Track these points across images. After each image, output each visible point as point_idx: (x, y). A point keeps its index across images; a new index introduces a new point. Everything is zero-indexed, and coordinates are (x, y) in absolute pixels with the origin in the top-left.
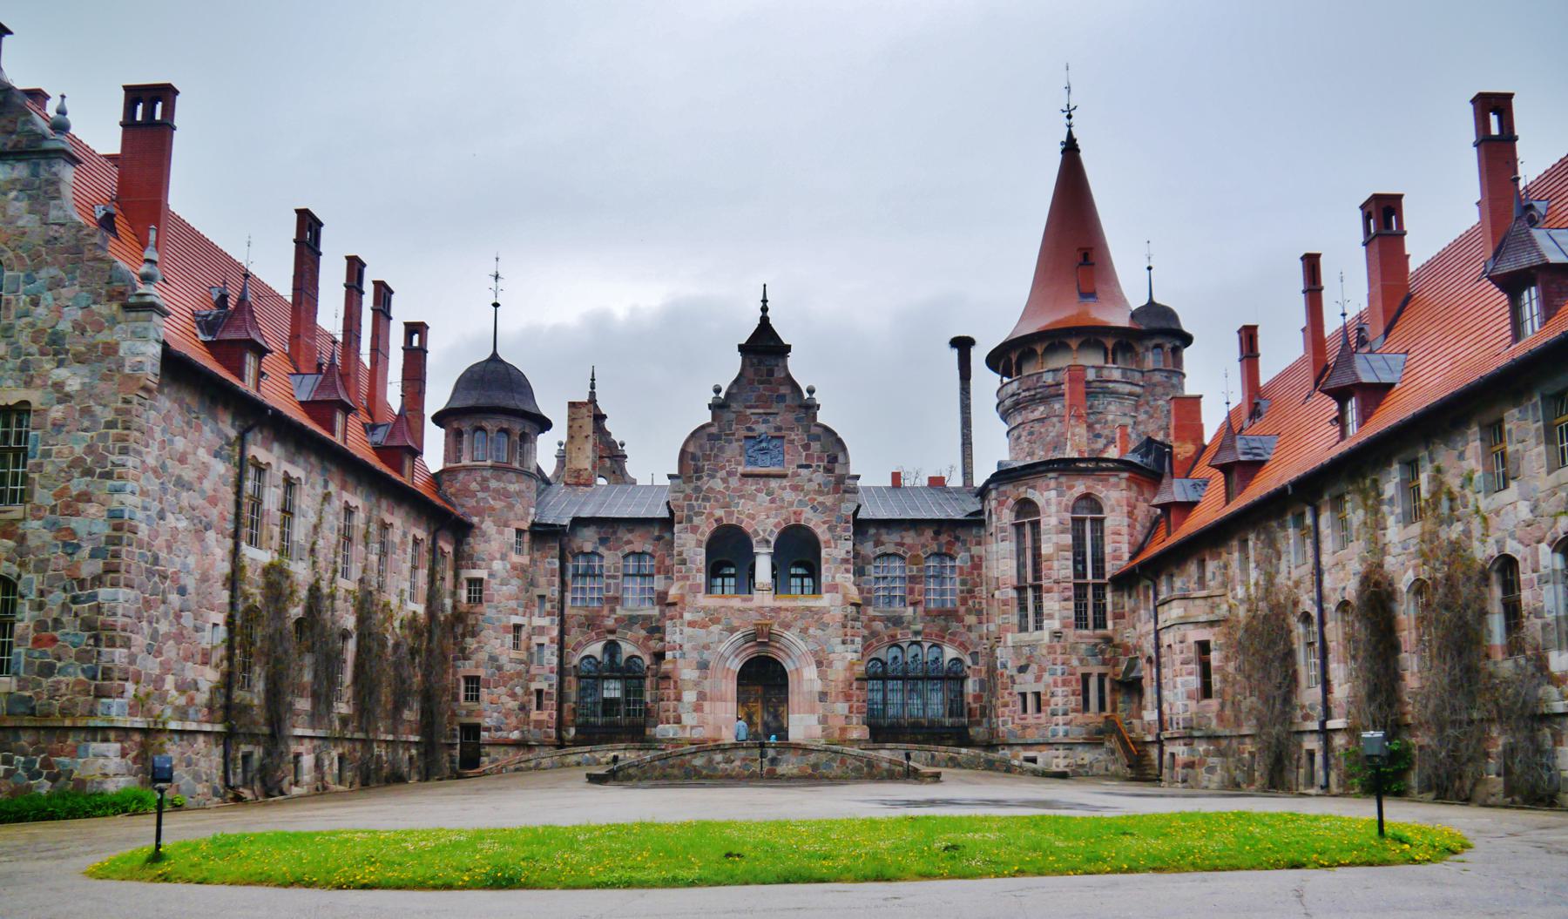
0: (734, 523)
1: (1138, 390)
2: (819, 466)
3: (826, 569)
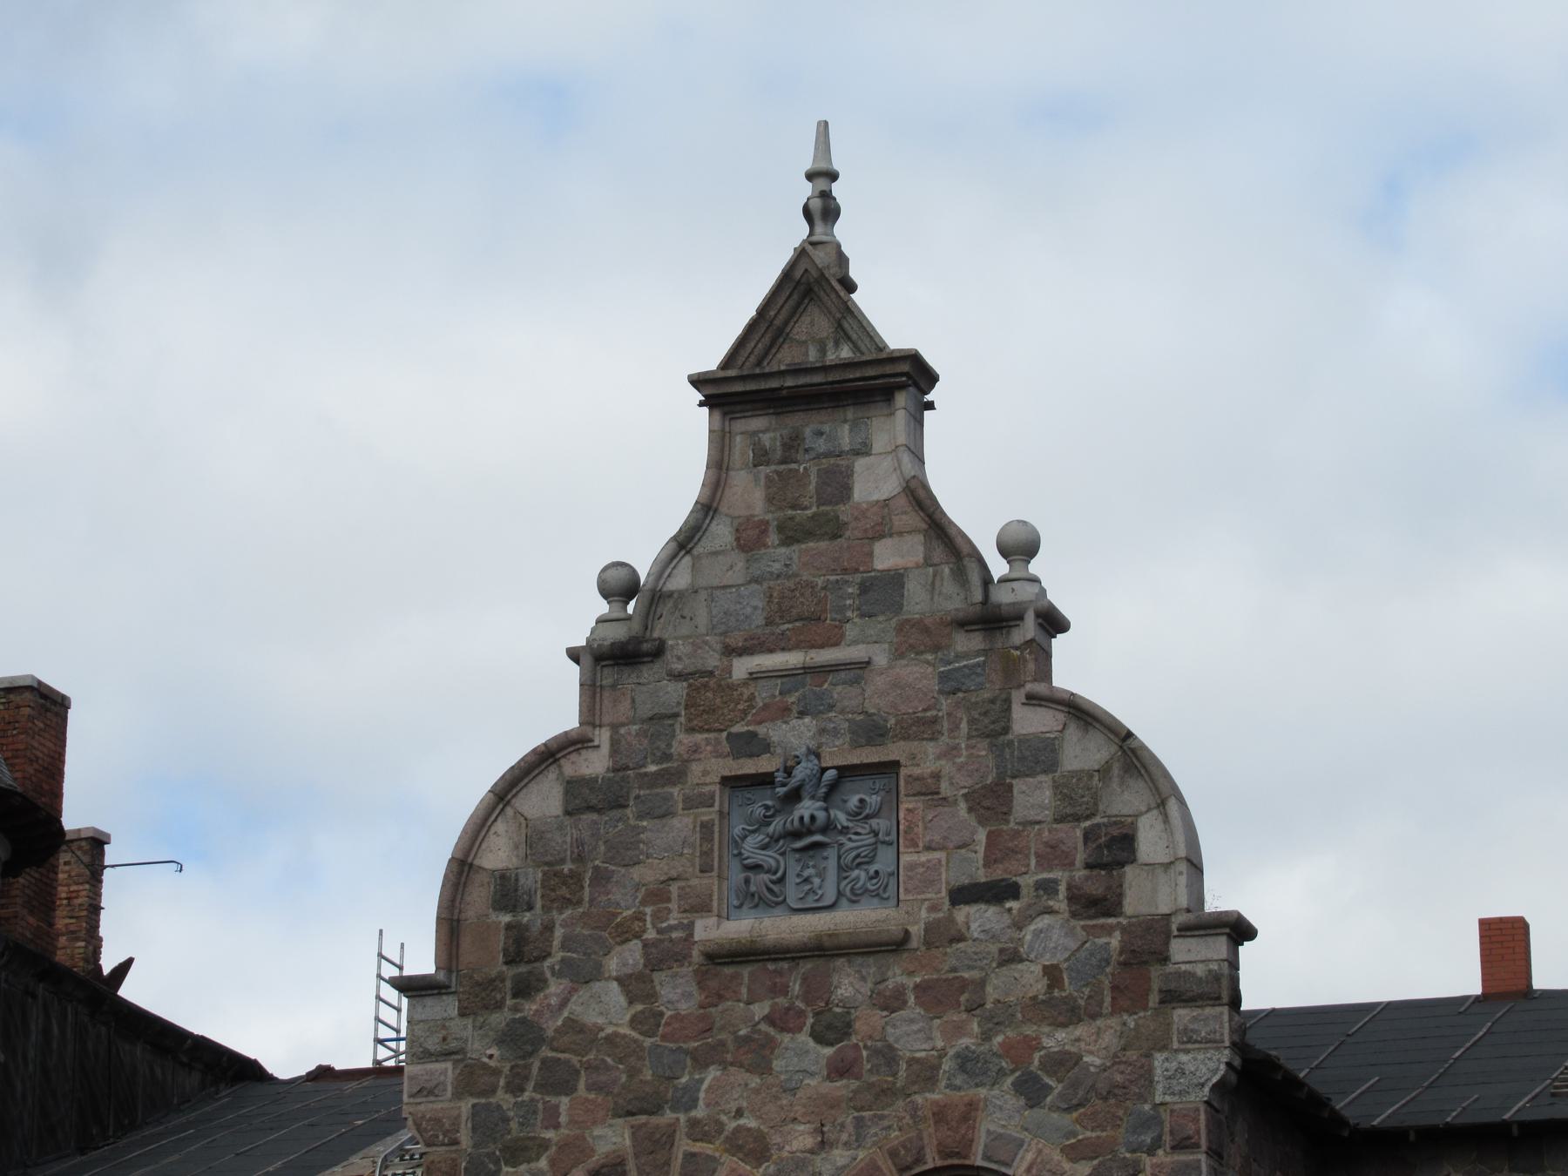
2: (1048, 887)
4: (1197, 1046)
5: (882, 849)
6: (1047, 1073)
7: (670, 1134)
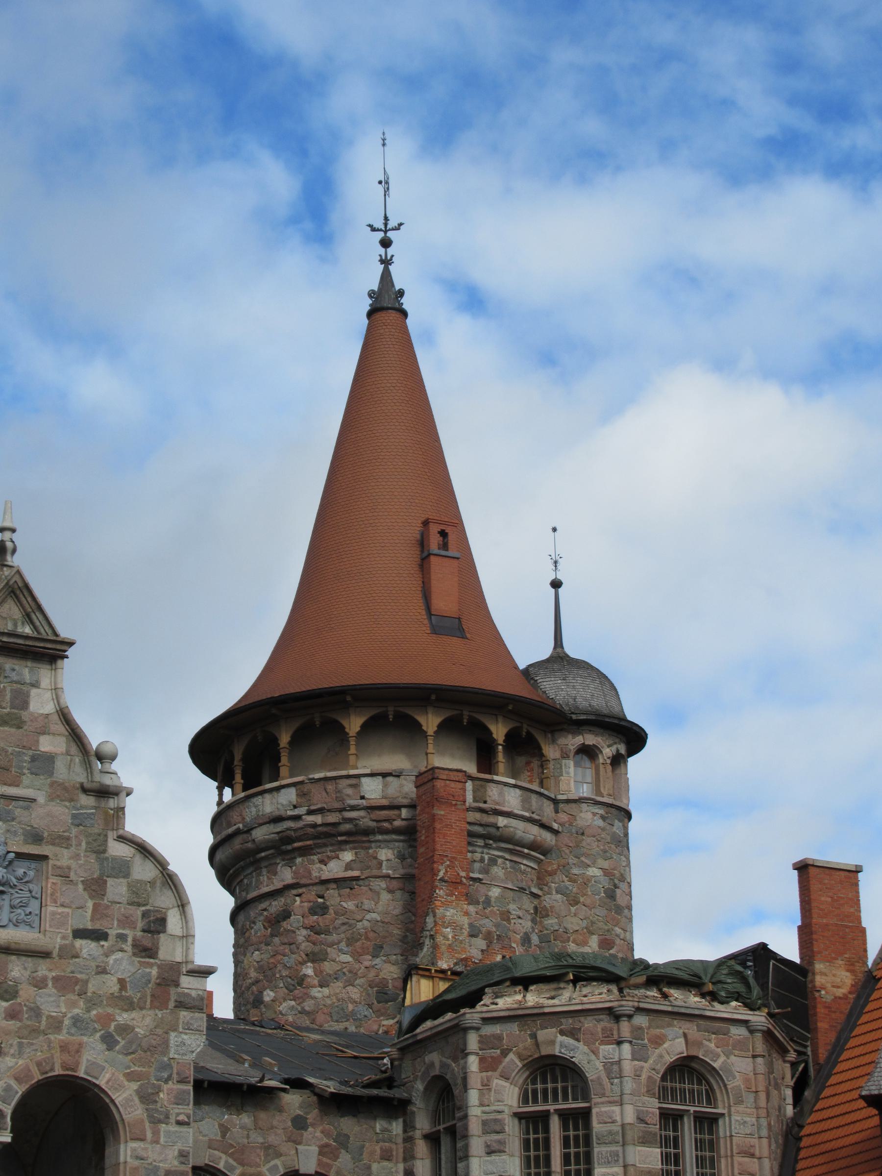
1: (547, 837)
2: (122, 937)
4: (191, 1031)
5: (33, 900)
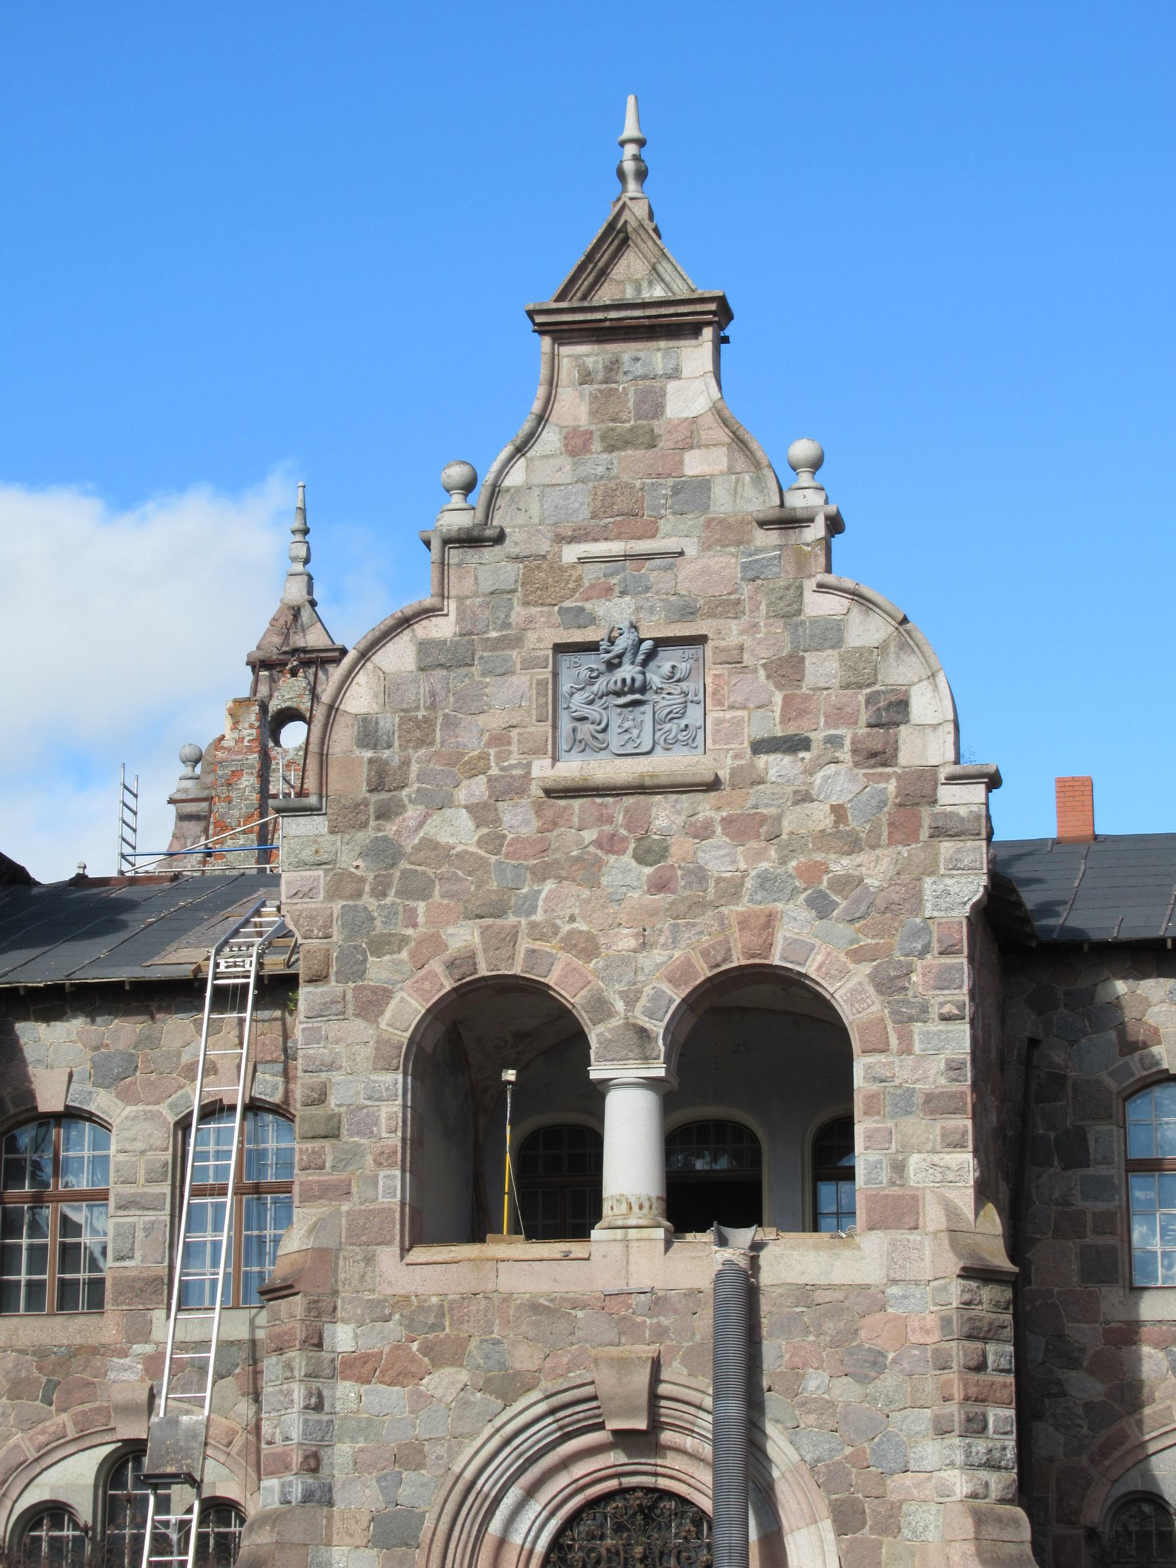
0: (517, 970)
2: (834, 741)
3: (869, 1137)
4: (960, 872)
6: (834, 891)
7: (513, 936)
